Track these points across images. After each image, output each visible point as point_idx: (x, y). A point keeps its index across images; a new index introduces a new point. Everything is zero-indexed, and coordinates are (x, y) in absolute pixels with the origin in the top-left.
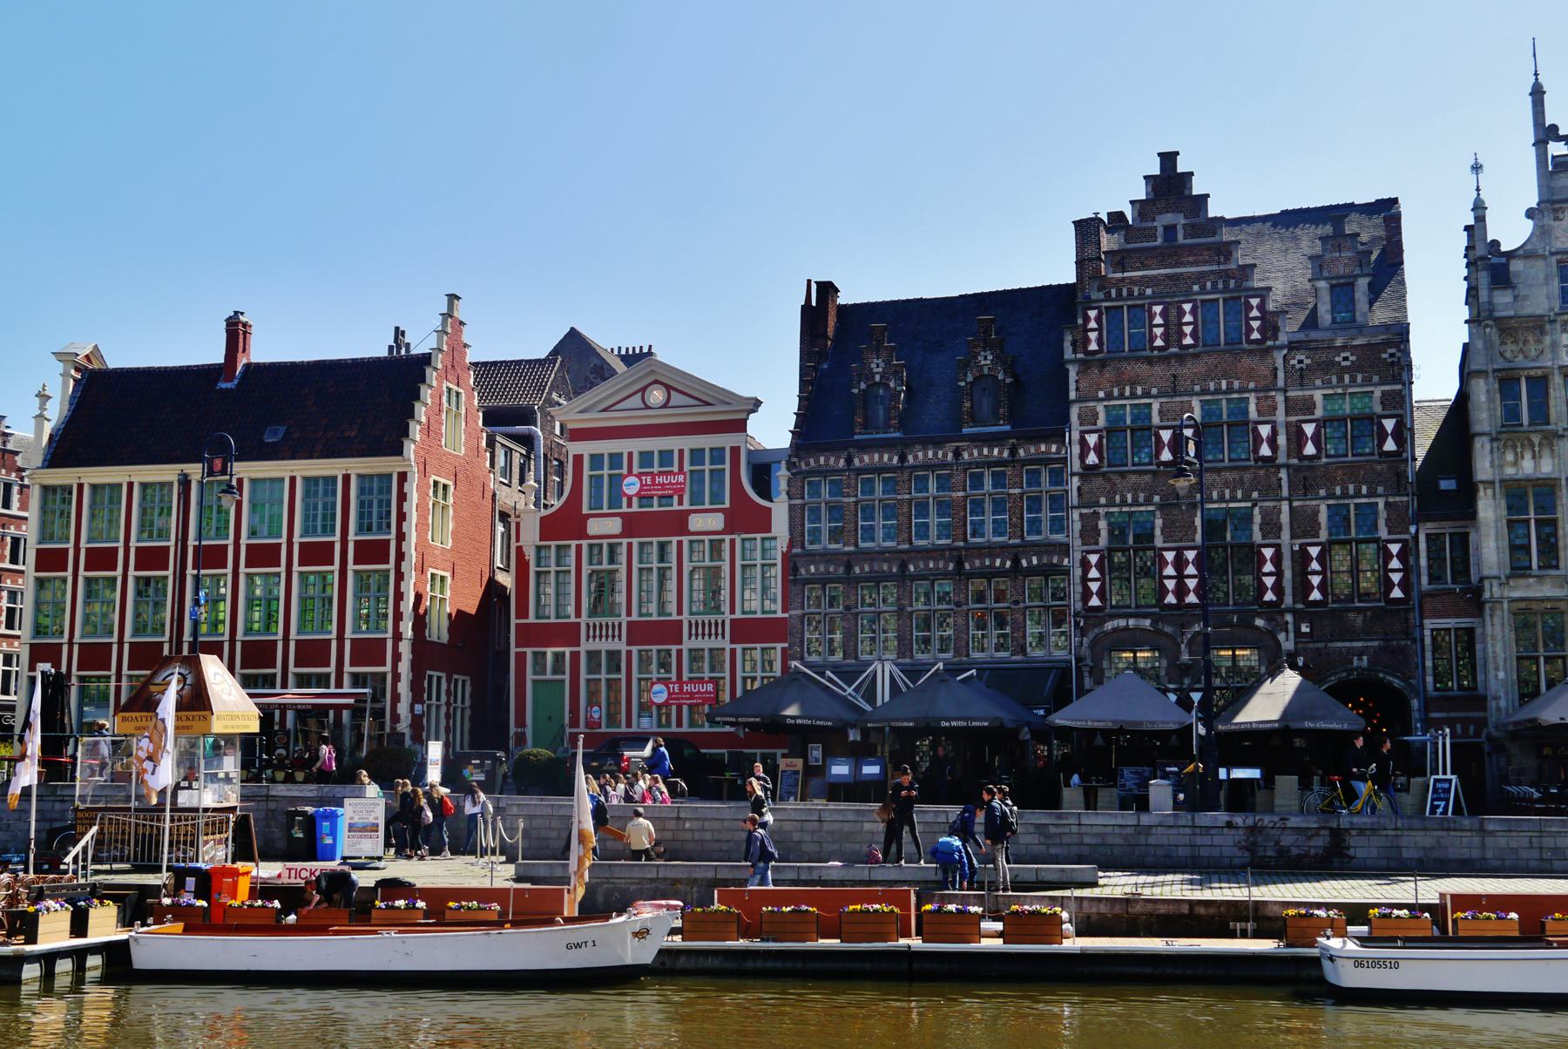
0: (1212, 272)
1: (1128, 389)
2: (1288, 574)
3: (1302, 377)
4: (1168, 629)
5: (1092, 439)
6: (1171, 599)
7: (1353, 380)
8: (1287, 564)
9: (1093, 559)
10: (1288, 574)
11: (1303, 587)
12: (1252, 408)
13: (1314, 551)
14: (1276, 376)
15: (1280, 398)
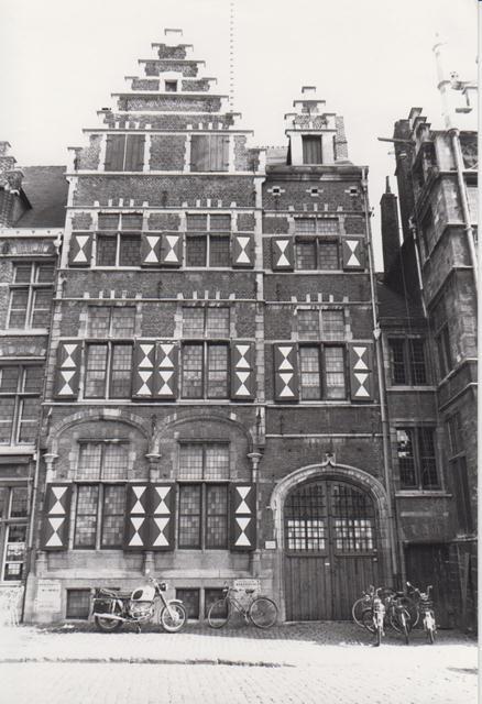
0: (205, 117)
1: (121, 200)
2: (261, 370)
3: (276, 202)
4: (139, 420)
5: (82, 241)
6: (144, 391)
7: (321, 208)
8: (260, 361)
9: (70, 349)
10: (261, 370)
11: (273, 384)
12: (234, 223)
13: (285, 351)
14: (254, 199)
15: (258, 215)
